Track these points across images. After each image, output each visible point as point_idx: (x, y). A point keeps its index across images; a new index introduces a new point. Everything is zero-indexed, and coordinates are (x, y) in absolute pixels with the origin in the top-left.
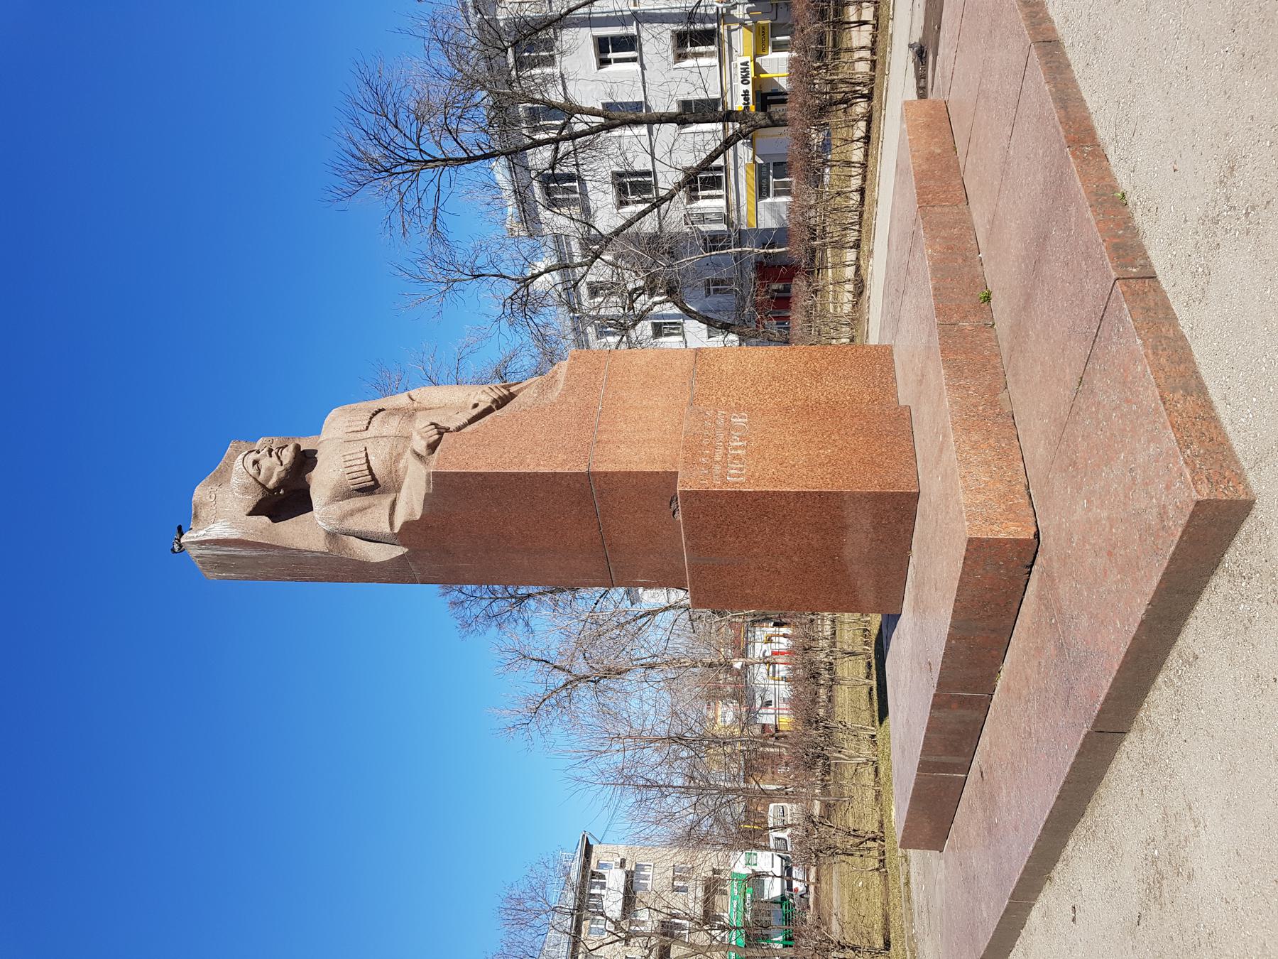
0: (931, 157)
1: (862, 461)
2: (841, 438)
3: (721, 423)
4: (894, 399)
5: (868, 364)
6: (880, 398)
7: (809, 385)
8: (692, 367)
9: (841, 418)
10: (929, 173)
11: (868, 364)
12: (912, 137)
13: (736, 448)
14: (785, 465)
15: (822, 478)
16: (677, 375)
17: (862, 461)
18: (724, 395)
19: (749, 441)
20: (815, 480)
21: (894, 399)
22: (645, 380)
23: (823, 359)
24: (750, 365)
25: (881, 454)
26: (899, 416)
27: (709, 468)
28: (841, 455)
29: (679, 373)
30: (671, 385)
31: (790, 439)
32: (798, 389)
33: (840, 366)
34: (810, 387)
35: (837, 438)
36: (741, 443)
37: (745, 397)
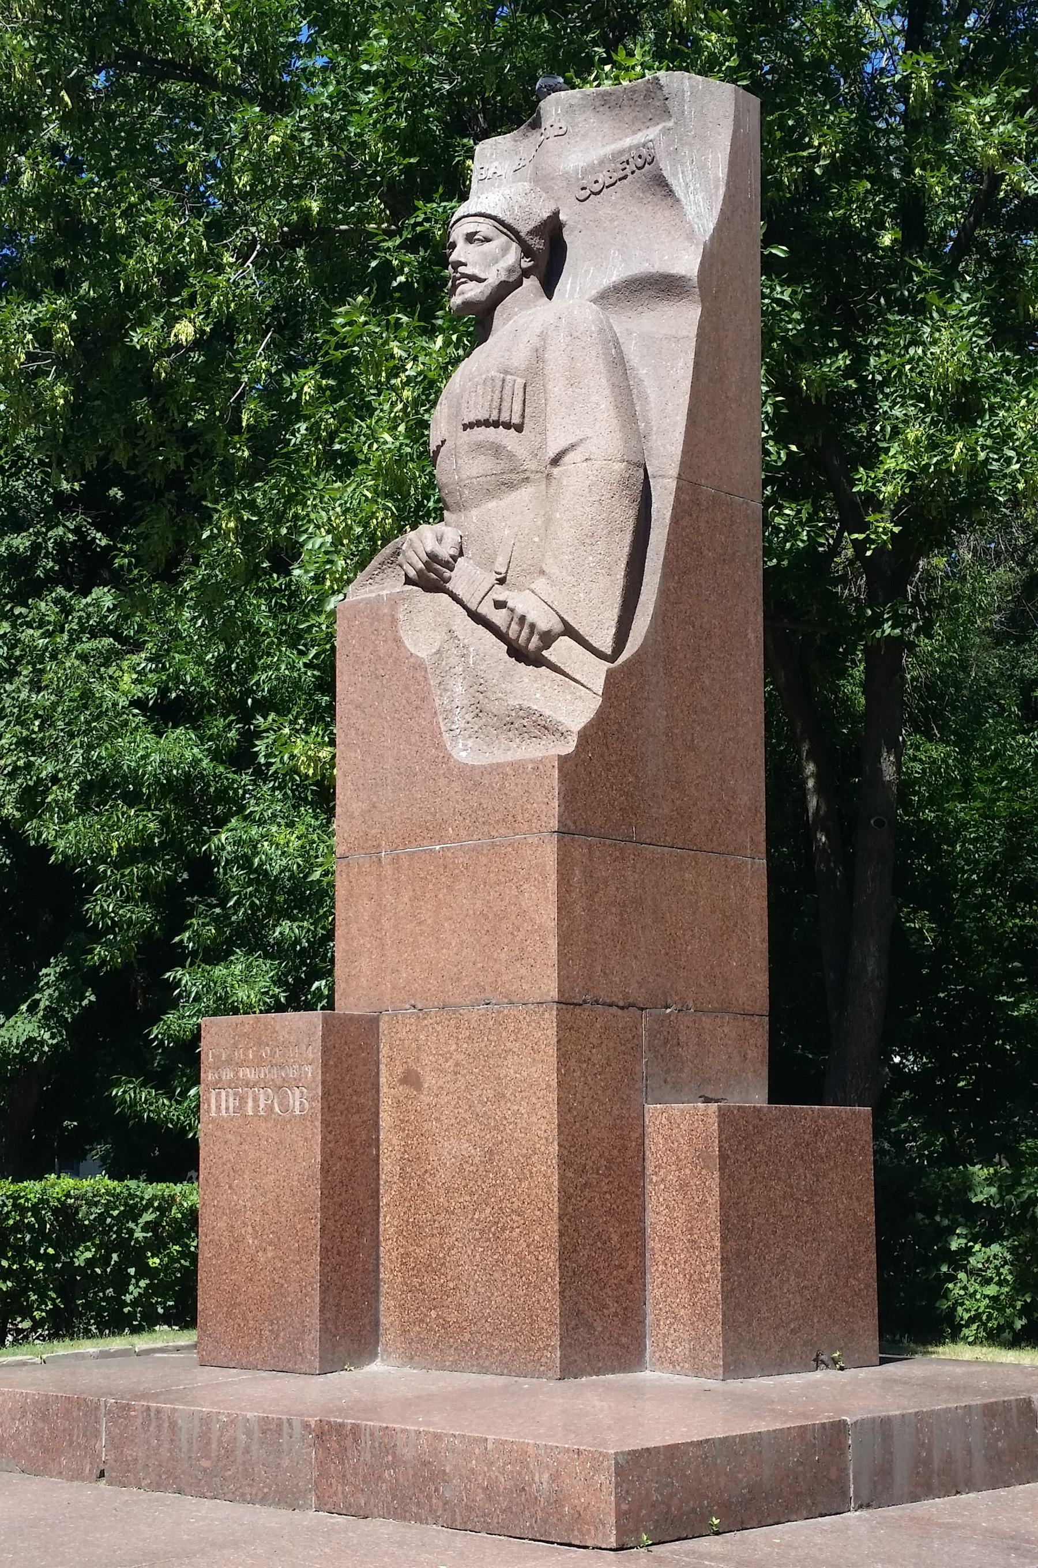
0: (438, 1476)
1: (236, 1288)
2: (268, 1261)
3: (293, 1073)
4: (448, 1363)
5: (517, 1329)
6: (451, 1340)
7: (476, 1216)
8: (515, 999)
9: (298, 1263)
10: (390, 1458)
11: (517, 1329)
12: (490, 1446)
13: (256, 1100)
14: (232, 1174)
15: (213, 1228)
16: (499, 974)
17: (236, 1288)
18: (457, 1065)
19: (266, 1119)
20: (212, 1218)
21: (448, 1363)
22: (491, 916)
23: (528, 1246)
24: (516, 1108)
25: (244, 1319)
26: (300, 1354)
27: (229, 1062)
28: (244, 1259)
29: (505, 978)
30: (480, 965)
31: (269, 1181)
32: (468, 1198)
33: (513, 1275)
34: (472, 1219)
35: (270, 1255)
36: (262, 1106)
37: (453, 1103)
